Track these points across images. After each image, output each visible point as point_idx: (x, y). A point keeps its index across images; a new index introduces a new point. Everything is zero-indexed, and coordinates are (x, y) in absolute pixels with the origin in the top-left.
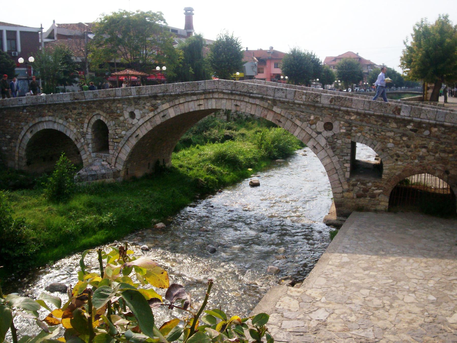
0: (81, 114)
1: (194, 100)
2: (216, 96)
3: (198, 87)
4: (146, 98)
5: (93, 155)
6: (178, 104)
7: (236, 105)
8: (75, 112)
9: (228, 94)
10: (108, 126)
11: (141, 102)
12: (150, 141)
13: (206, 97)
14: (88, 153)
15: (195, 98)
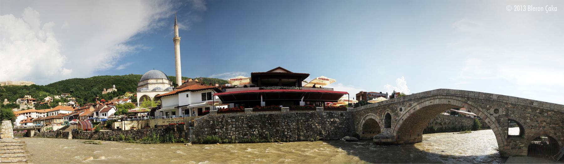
0: (381, 111)
1: (428, 100)
2: (439, 97)
3: (431, 93)
4: (407, 101)
5: (385, 129)
6: (421, 103)
7: (449, 101)
8: (379, 110)
9: (445, 96)
10: (391, 115)
11: (405, 103)
12: (410, 123)
13: (434, 98)
14: (383, 128)
15: (429, 99)
